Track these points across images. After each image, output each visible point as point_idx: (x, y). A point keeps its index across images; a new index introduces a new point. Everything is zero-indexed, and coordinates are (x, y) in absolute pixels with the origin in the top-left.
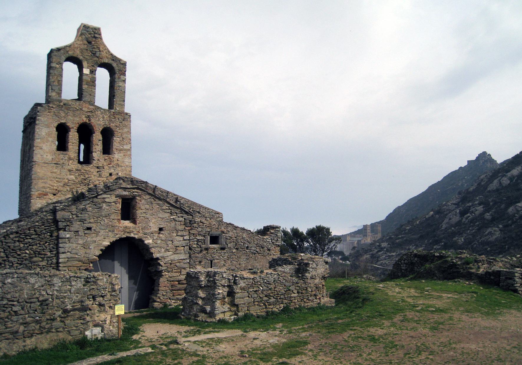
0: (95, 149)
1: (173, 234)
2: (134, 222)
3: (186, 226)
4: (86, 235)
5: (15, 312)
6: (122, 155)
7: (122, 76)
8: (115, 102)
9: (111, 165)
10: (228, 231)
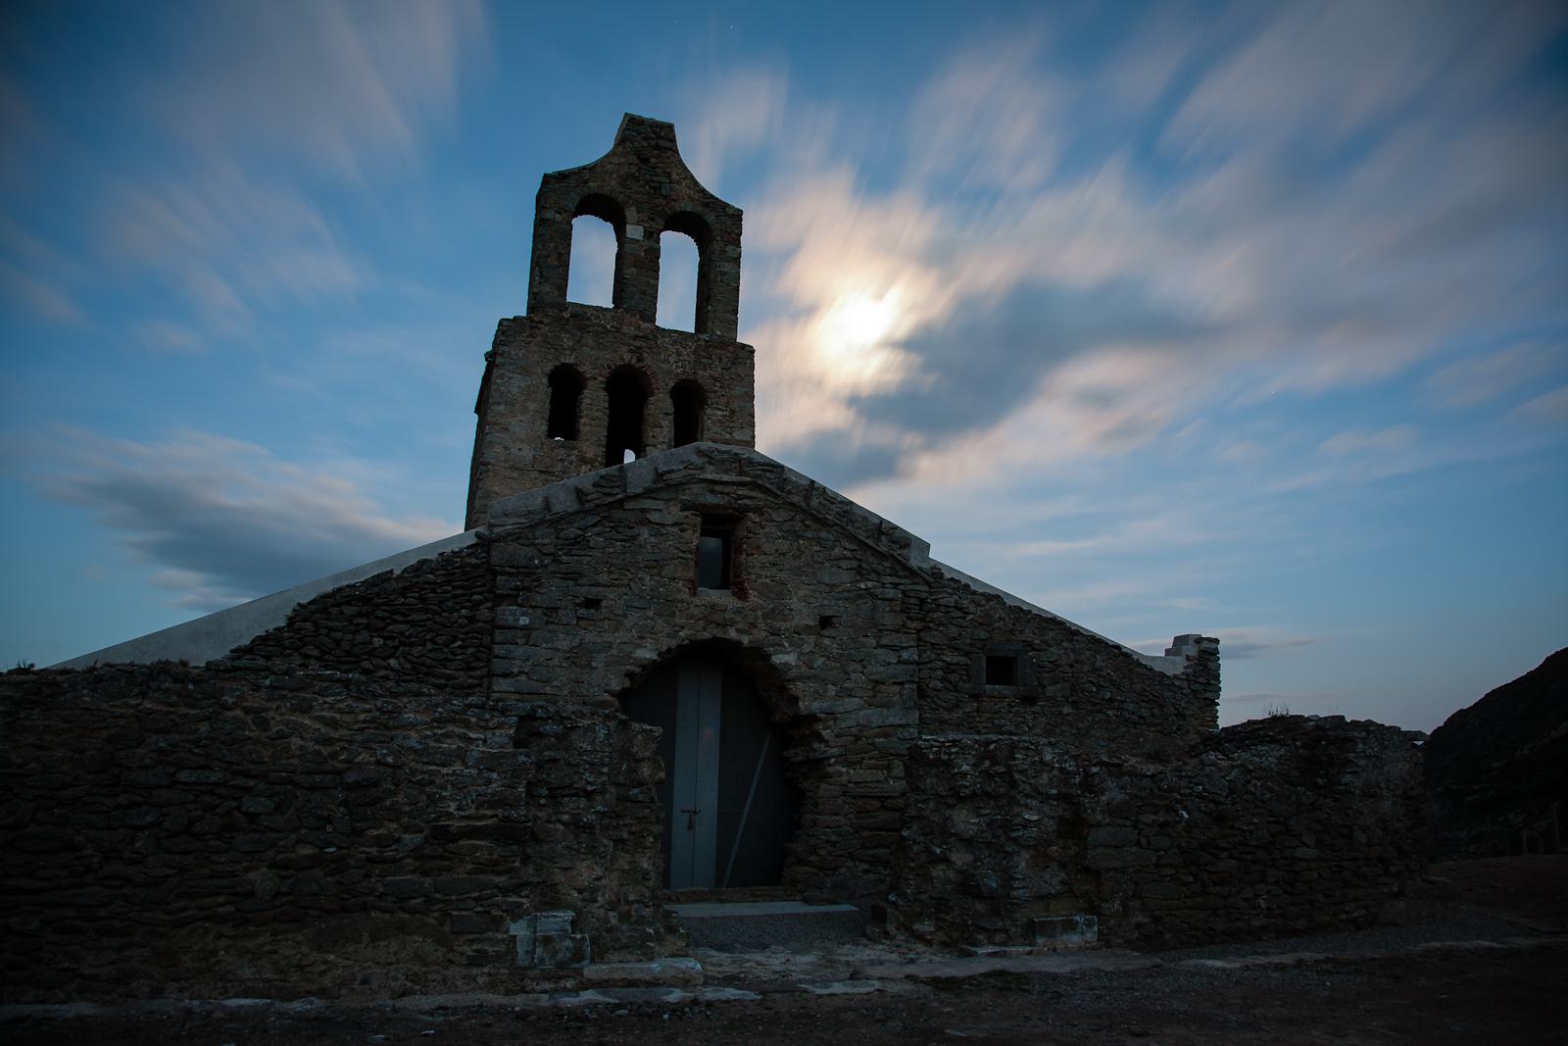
0: (653, 437)
1: (864, 640)
2: (741, 594)
3: (908, 618)
4: (583, 623)
5: (252, 817)
7: (729, 248)
8: (710, 315)
10: (1046, 642)
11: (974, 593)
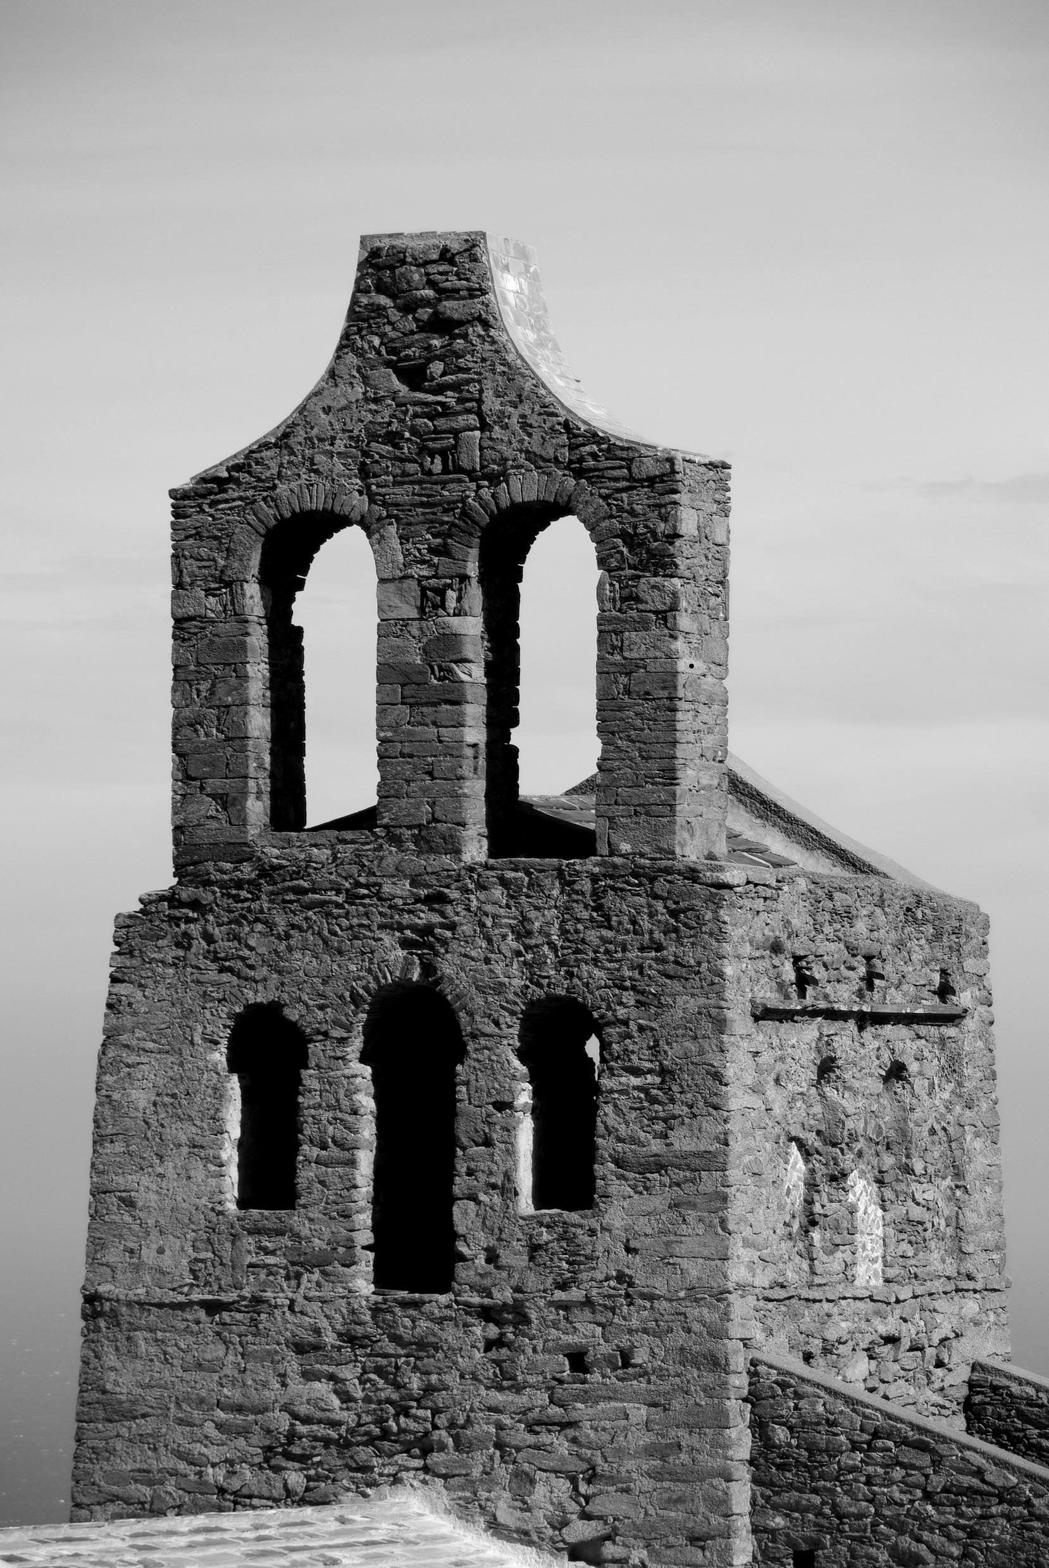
0: (470, 1173)
6: (657, 1202)
7: (648, 580)
9: (575, 1294)
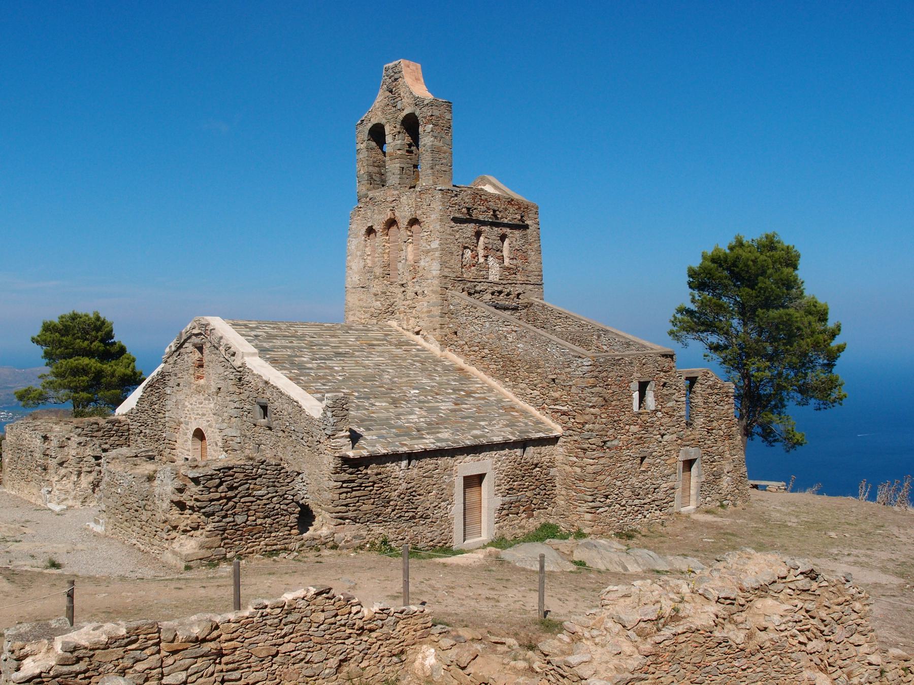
9: (415, 280)
11: (254, 375)
